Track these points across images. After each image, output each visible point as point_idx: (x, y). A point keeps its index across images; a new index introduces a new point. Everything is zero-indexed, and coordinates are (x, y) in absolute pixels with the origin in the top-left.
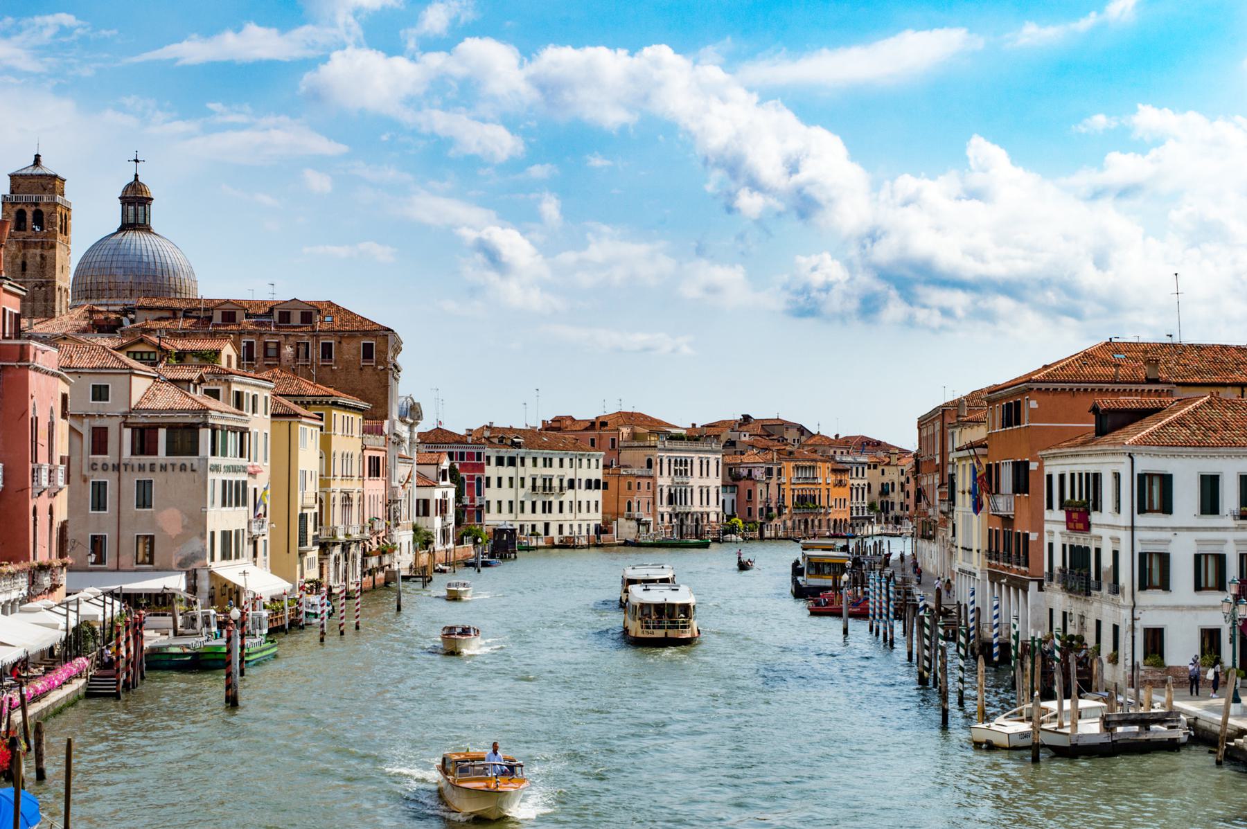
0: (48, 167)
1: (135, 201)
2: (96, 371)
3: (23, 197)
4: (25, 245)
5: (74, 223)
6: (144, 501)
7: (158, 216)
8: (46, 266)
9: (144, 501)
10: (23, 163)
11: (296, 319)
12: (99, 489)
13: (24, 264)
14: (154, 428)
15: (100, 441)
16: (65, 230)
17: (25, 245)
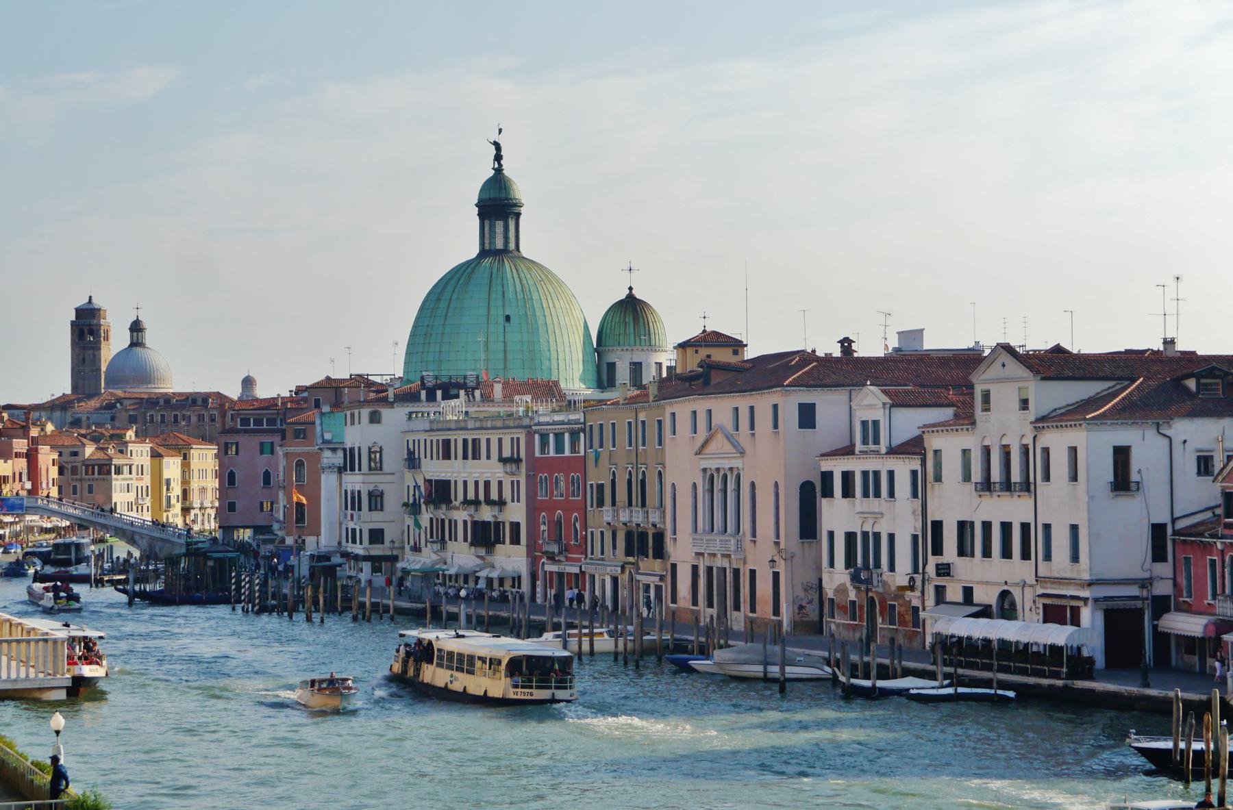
0: (97, 302)
1: (136, 327)
2: (73, 446)
3: (82, 322)
4: (84, 349)
5: (111, 334)
6: (90, 491)
7: (149, 338)
8: (96, 359)
9: (90, 491)
10: (82, 301)
11: (200, 402)
12: (75, 487)
13: (84, 360)
14: (93, 466)
15: (74, 471)
16: (107, 338)
17: (84, 349)
